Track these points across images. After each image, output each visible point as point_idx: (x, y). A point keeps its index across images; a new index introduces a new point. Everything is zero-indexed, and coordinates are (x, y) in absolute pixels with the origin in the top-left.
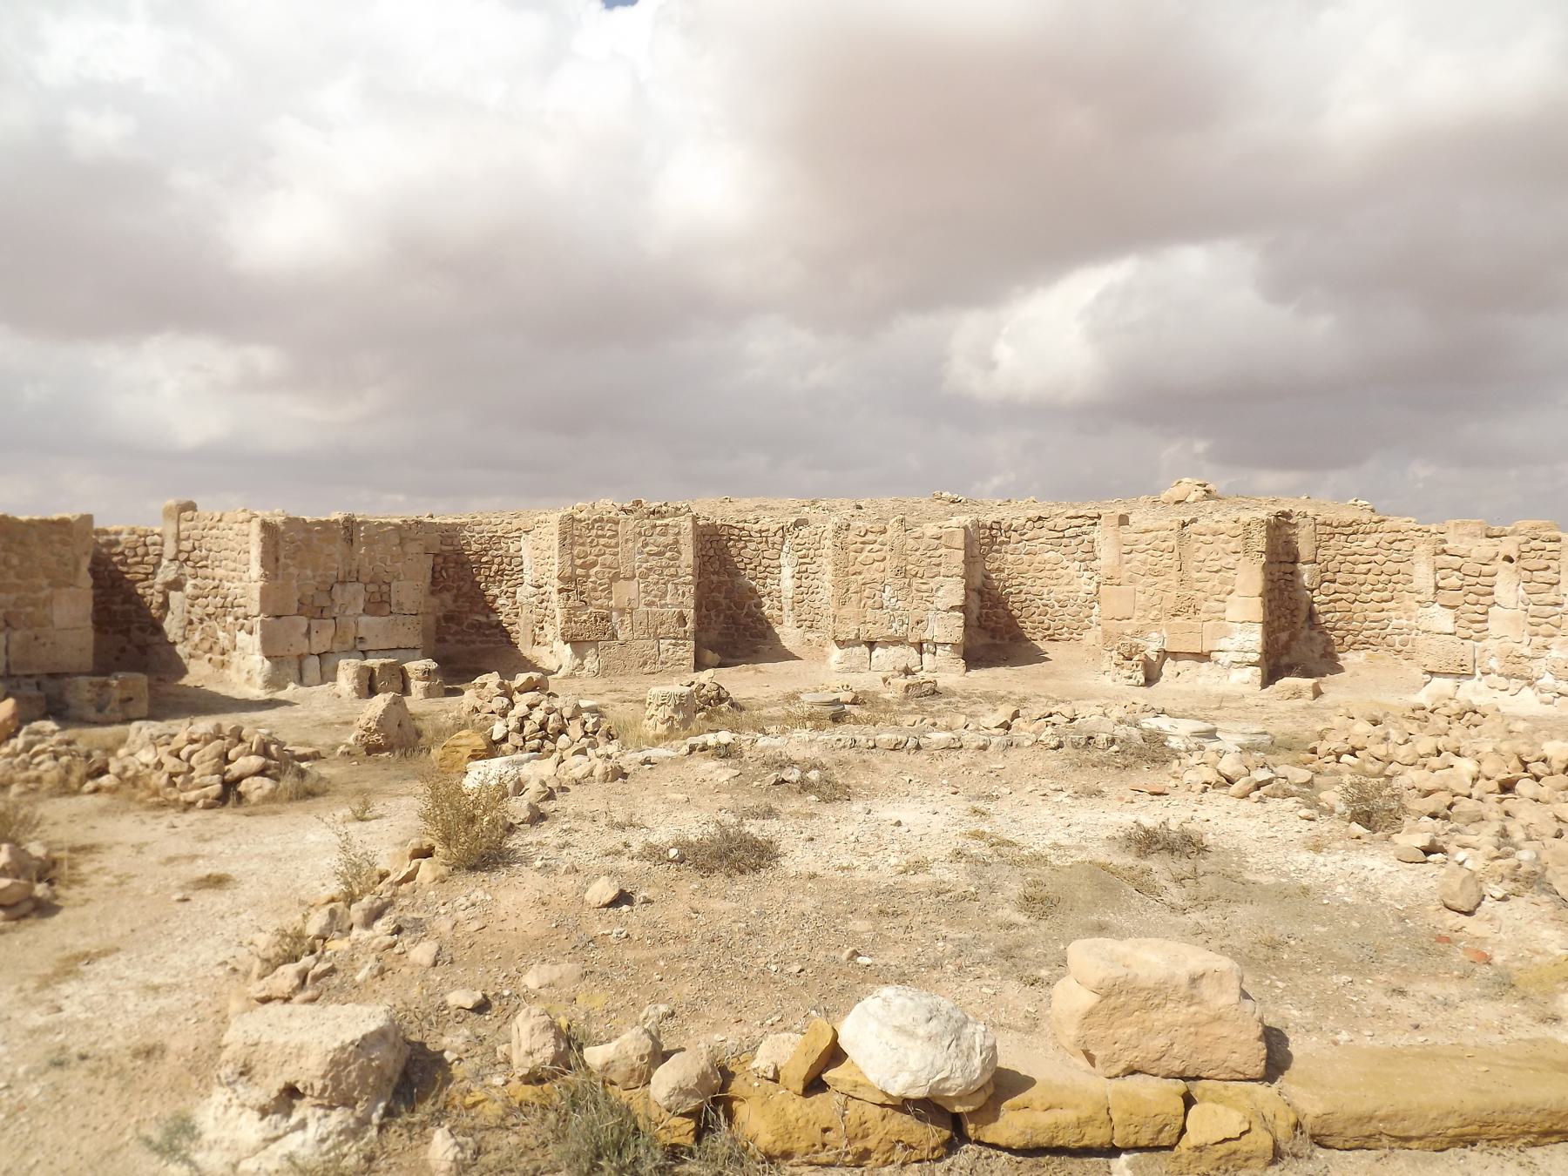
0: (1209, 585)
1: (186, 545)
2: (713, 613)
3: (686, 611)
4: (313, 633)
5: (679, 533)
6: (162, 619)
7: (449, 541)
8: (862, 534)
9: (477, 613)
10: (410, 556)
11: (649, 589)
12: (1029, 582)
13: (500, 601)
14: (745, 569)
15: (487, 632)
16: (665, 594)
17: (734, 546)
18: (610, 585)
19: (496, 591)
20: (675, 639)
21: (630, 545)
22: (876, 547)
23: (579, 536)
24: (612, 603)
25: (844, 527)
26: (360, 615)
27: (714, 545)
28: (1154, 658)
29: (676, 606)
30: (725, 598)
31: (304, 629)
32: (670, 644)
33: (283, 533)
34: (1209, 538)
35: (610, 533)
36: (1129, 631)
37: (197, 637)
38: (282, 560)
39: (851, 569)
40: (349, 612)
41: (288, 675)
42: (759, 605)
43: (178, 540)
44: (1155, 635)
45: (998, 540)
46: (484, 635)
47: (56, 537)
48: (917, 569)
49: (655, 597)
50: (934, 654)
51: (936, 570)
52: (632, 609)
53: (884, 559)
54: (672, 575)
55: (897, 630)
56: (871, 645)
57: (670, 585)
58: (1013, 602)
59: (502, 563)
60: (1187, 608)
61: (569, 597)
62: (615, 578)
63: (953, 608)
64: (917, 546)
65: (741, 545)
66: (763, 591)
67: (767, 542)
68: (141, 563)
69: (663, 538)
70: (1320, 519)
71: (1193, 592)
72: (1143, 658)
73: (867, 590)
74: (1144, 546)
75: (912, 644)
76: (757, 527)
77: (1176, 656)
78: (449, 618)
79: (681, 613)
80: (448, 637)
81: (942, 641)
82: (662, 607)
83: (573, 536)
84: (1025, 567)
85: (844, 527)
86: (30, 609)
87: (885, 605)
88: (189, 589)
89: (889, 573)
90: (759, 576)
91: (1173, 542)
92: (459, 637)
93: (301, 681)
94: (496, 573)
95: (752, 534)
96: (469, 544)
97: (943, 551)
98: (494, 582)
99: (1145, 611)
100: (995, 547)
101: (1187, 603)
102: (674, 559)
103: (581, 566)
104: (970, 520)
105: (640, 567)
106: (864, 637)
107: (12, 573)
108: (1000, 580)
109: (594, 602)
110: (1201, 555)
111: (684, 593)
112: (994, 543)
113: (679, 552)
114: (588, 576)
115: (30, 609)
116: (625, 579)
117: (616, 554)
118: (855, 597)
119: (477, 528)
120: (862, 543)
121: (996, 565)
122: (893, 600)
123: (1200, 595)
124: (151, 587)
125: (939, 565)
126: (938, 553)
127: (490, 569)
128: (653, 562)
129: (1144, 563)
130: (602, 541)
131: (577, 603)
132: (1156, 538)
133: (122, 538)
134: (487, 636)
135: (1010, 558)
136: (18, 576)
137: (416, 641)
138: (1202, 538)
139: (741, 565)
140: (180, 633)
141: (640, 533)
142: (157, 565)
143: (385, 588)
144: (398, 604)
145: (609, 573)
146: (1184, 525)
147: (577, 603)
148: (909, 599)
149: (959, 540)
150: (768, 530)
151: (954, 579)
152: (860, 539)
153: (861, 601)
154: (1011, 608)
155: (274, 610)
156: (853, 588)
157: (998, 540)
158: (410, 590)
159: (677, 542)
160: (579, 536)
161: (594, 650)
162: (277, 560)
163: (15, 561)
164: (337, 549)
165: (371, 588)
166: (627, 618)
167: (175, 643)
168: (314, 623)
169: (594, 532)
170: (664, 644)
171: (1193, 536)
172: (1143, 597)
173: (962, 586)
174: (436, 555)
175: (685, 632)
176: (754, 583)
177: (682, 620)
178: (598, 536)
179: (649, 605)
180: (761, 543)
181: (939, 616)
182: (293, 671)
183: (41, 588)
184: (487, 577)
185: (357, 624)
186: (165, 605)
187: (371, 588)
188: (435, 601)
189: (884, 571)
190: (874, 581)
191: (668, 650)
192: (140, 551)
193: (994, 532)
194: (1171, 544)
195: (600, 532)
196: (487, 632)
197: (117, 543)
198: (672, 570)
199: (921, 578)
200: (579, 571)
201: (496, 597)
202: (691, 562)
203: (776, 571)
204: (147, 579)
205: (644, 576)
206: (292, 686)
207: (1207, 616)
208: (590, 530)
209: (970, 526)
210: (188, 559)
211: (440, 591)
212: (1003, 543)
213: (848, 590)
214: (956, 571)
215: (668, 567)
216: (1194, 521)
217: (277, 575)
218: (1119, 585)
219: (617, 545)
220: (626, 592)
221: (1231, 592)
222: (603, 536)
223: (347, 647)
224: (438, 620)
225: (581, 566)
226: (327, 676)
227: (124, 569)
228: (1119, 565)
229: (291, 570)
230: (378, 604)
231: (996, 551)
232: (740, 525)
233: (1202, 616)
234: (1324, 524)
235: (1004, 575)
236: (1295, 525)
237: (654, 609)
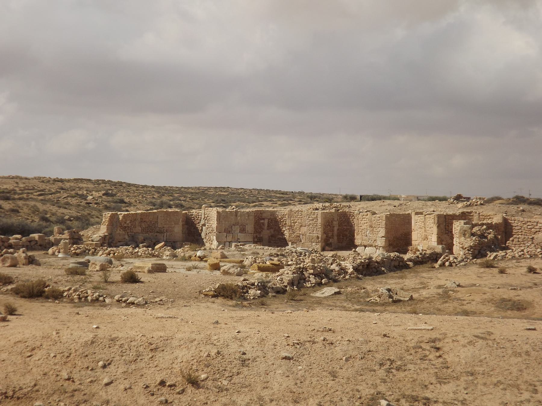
1: (206, 216)
2: (345, 238)
3: (319, 235)
5: (317, 215)
7: (273, 215)
9: (280, 235)
13: (285, 232)
15: (282, 241)
16: (313, 231)
18: (300, 228)
19: (284, 229)
21: (305, 217)
22: (365, 219)
23: (293, 215)
27: (345, 218)
29: (317, 234)
30: (349, 233)
36: (417, 244)
37: (207, 238)
38: (221, 220)
39: (360, 225)
40: (236, 232)
43: (205, 214)
44: (421, 245)
46: (281, 241)
47: (175, 215)
51: (379, 226)
53: (367, 223)
56: (365, 246)
61: (290, 231)
62: (301, 226)
63: (383, 237)
65: (353, 217)
68: (198, 220)
70: (481, 214)
78: (272, 236)
79: (318, 236)
80: (272, 241)
81: (380, 246)
82: (313, 234)
88: (206, 226)
89: (368, 227)
91: (423, 220)
92: (274, 241)
96: (278, 216)
97: (380, 221)
103: (293, 223)
106: (362, 244)
113: (317, 220)
114: (295, 225)
116: (304, 226)
117: (302, 220)
119: (280, 212)
124: (199, 225)
125: (380, 225)
126: (380, 221)
128: (311, 222)
130: (298, 216)
134: (282, 241)
142: (201, 220)
143: (244, 227)
144: (247, 231)
146: (425, 216)
149: (384, 218)
152: (362, 217)
155: (219, 231)
158: (250, 228)
159: (317, 217)
160: (293, 215)
164: (233, 218)
166: (304, 237)
167: (203, 239)
168: (228, 234)
169: (296, 214)
170: (314, 244)
172: (419, 235)
174: (269, 219)
177: (318, 237)
179: (310, 233)
183: (173, 224)
186: (202, 230)
187: (241, 227)
188: (268, 231)
192: (197, 217)
196: (282, 241)
197: (193, 215)
198: (316, 224)
200: (292, 224)
201: (284, 231)
202: (320, 222)
204: (198, 224)
205: (309, 226)
210: (206, 219)
211: (270, 229)
213: (359, 231)
214: (383, 226)
215: (315, 223)
217: (220, 223)
219: (302, 218)
220: (304, 230)
221: (432, 234)
222: (299, 215)
224: (269, 237)
225: (293, 223)
226: (230, 246)
227: (194, 221)
229: (223, 222)
230: (243, 230)
232: (353, 212)
234: (482, 215)
236: (473, 216)
237: (311, 234)
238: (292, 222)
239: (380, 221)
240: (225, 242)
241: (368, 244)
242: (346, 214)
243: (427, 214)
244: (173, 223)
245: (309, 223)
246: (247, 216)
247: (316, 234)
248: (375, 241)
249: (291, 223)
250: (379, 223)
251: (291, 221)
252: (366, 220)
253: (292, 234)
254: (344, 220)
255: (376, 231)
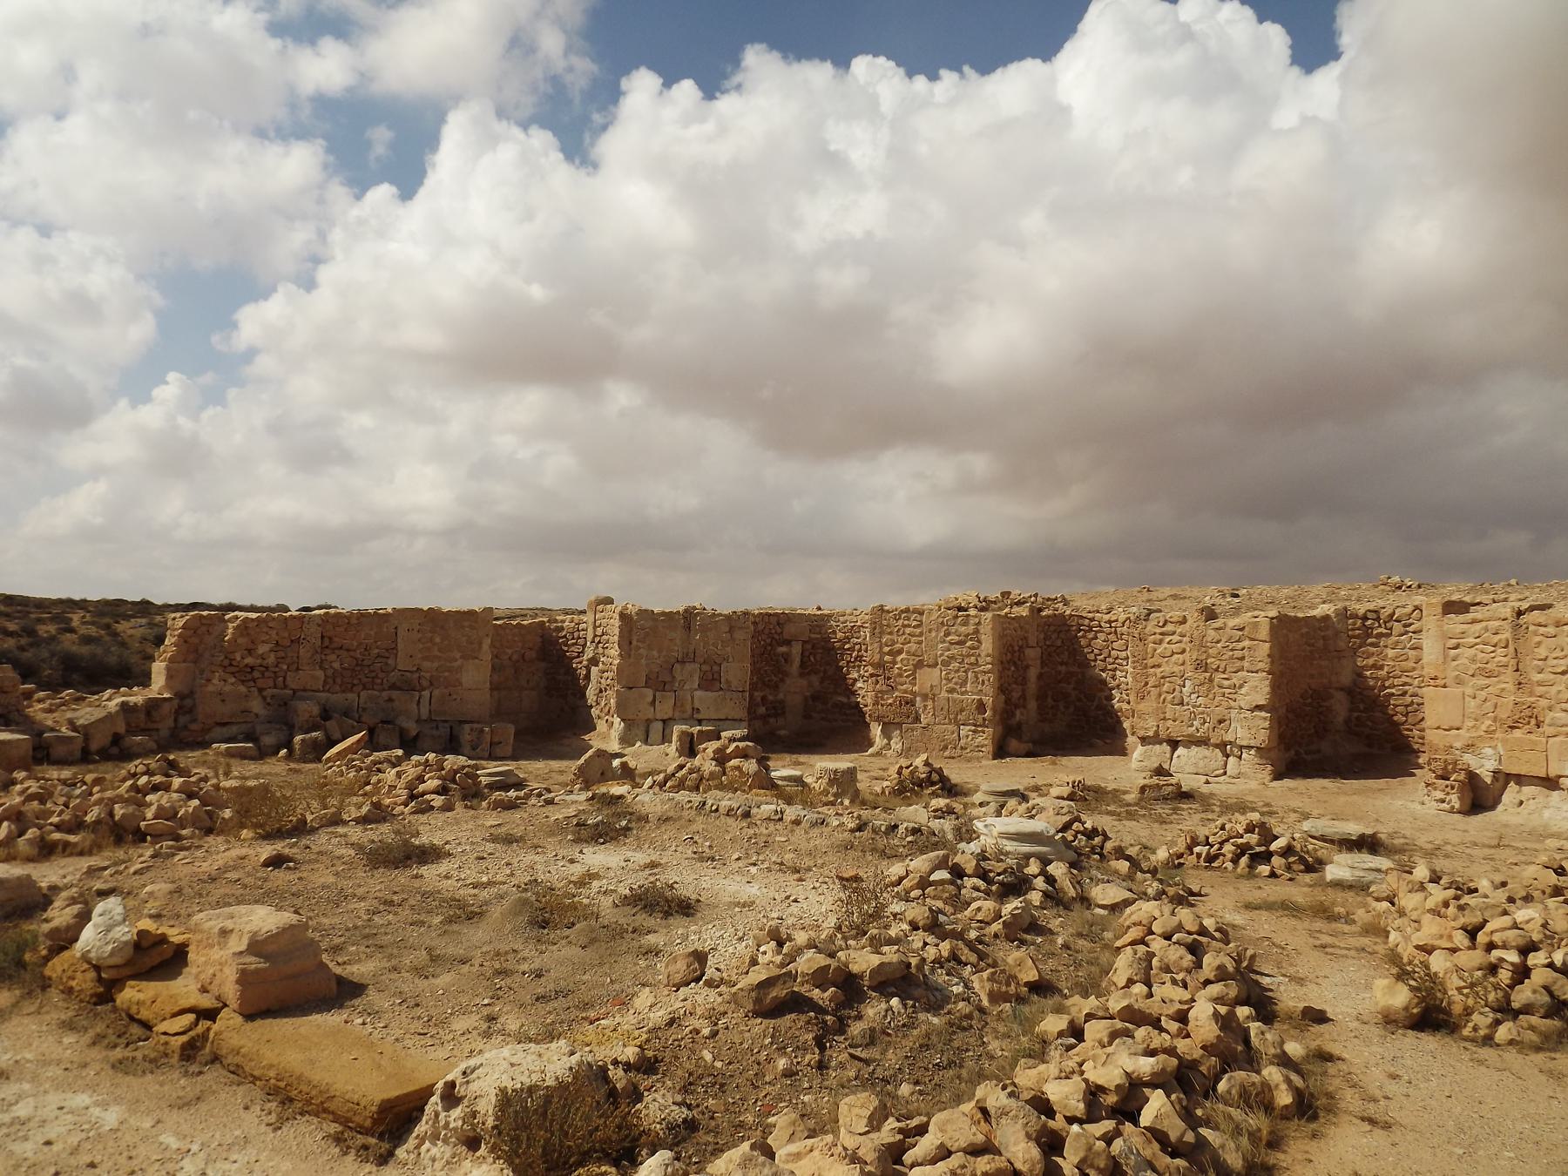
0: (1554, 690)
1: (599, 631)
2: (1061, 705)
4: (657, 702)
5: (979, 623)
6: (586, 687)
7: (818, 629)
8: (1161, 624)
9: (840, 694)
10: (737, 642)
11: (950, 676)
12: (1416, 682)
13: (859, 684)
14: (1095, 660)
17: (1082, 637)
18: (914, 673)
19: (855, 675)
20: (975, 725)
21: (933, 634)
22: (1176, 638)
24: (916, 688)
25: (1142, 617)
26: (696, 690)
27: (1062, 635)
28: (1488, 780)
29: (977, 694)
30: (1074, 689)
31: (650, 699)
32: (970, 731)
33: (637, 621)
34: (1551, 630)
35: (915, 623)
36: (1458, 745)
38: (634, 643)
39: (1150, 662)
40: (686, 687)
41: (637, 735)
42: (1110, 697)
43: (595, 627)
44: (1489, 751)
45: (1375, 632)
46: (845, 714)
47: (466, 624)
48: (1218, 662)
49: (956, 684)
50: (1240, 757)
51: (1239, 664)
52: (934, 695)
53: (1183, 651)
54: (971, 664)
55: (1197, 728)
56: (1174, 744)
57: (970, 674)
58: (1396, 706)
59: (860, 650)
60: (1527, 718)
61: (877, 682)
62: (919, 665)
63: (1259, 708)
64: (1218, 637)
65: (1091, 635)
66: (1113, 684)
67: (1116, 632)
68: (576, 644)
69: (964, 628)
71: (1533, 699)
72: (1462, 776)
73: (1167, 684)
74: (1472, 640)
75: (1216, 746)
76: (1107, 617)
77: (1520, 779)
78: (815, 698)
80: (814, 715)
81: (1244, 743)
82: (962, 694)
83: (882, 626)
84: (1411, 664)
85: (1142, 617)
86: (446, 674)
87: (1185, 701)
89: (1189, 667)
90: (1109, 667)
91: (1506, 635)
92: (824, 715)
93: (646, 742)
94: (856, 659)
95: (1103, 624)
96: (834, 632)
97: (1246, 643)
98: (854, 667)
99: (1476, 720)
100: (1370, 640)
101: (1528, 712)
102: (974, 648)
103: (889, 653)
104: (1332, 610)
105: (942, 655)
107: (436, 648)
108: (1377, 679)
109: (899, 687)
110: (1542, 652)
111: (983, 681)
112: (1369, 636)
113: (979, 642)
114: (895, 663)
115: (446, 674)
116: (929, 666)
117: (920, 643)
118: (1154, 692)
119: (842, 619)
120: (1161, 634)
121: (1371, 661)
122: (1194, 696)
123: (1544, 703)
124: (581, 663)
125: (1242, 658)
126: (1241, 645)
127: (851, 655)
128: (955, 650)
129: (1473, 661)
130: (908, 630)
131: (884, 688)
132: (1486, 629)
133: (565, 625)
135: (1391, 653)
136: (439, 651)
137: (743, 714)
138: (1542, 630)
139: (1091, 657)
140: (595, 698)
141: (942, 623)
142: (584, 646)
143: (716, 668)
144: (728, 682)
145: (914, 660)
146: (1520, 613)
147: (884, 688)
148: (1211, 696)
149: (1264, 632)
150: (1117, 621)
151: (1260, 674)
152: (1158, 630)
153: (1160, 695)
154: (1391, 712)
156: (1152, 681)
157: (1375, 632)
158: (737, 672)
159: (977, 632)
161: (898, 732)
162: (631, 643)
163: (438, 640)
164: (678, 635)
165: (705, 668)
166: (930, 703)
167: (591, 707)
168: (657, 693)
169: (900, 622)
170: (964, 730)
171: (1532, 628)
172: (1473, 703)
173: (1267, 682)
174: (804, 642)
175: (984, 719)
176: (1104, 675)
177: (981, 707)
178: (905, 626)
179: (951, 691)
180: (1110, 633)
181: (1242, 716)
182: (641, 732)
183: (456, 660)
184: (848, 662)
185: (692, 698)
186: (588, 677)
187: (705, 668)
188: (804, 682)
189: (1183, 664)
190: (1172, 674)
191: (967, 736)
192: (576, 635)
193: (1369, 622)
194: (1503, 637)
195: (906, 622)
197: (562, 629)
198: (973, 659)
199: (1224, 672)
200: (887, 658)
201: (855, 680)
202: (990, 651)
203: (1125, 663)
204: (578, 657)
205: (946, 664)
206: (638, 744)
207: (1549, 730)
208: (897, 620)
209: (1333, 615)
211: (809, 674)
212: (1380, 635)
213: (1147, 684)
214: (1261, 665)
215: (969, 656)
216: (1543, 608)
217: (630, 656)
218: (1445, 686)
219: (921, 634)
220: (930, 678)
222: (909, 626)
223: (686, 715)
224: (806, 699)
225: (889, 653)
227: (566, 649)
228: (1444, 663)
230: (710, 681)
231: (1373, 645)
232: (1090, 615)
233: (1547, 729)
235: (1383, 673)
237: (955, 695)
238: (886, 649)
239: (1241, 645)
240: (649, 722)
241: (1189, 736)
242: (1065, 624)
243: (1532, 609)
244: (458, 655)
245: (947, 653)
246: (727, 629)
247: (973, 694)
248: (1220, 722)
249: (882, 654)
250: (1238, 654)
251: (881, 648)
252: (1180, 642)
253: (887, 692)
254: (1059, 643)
255: (1226, 683)
